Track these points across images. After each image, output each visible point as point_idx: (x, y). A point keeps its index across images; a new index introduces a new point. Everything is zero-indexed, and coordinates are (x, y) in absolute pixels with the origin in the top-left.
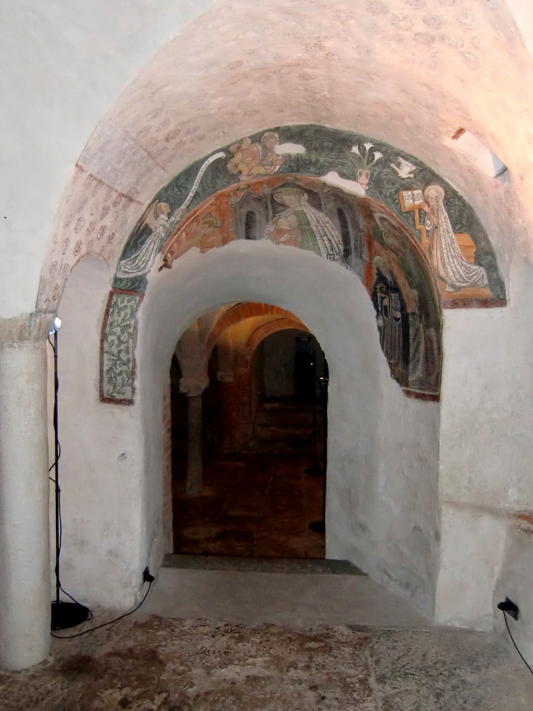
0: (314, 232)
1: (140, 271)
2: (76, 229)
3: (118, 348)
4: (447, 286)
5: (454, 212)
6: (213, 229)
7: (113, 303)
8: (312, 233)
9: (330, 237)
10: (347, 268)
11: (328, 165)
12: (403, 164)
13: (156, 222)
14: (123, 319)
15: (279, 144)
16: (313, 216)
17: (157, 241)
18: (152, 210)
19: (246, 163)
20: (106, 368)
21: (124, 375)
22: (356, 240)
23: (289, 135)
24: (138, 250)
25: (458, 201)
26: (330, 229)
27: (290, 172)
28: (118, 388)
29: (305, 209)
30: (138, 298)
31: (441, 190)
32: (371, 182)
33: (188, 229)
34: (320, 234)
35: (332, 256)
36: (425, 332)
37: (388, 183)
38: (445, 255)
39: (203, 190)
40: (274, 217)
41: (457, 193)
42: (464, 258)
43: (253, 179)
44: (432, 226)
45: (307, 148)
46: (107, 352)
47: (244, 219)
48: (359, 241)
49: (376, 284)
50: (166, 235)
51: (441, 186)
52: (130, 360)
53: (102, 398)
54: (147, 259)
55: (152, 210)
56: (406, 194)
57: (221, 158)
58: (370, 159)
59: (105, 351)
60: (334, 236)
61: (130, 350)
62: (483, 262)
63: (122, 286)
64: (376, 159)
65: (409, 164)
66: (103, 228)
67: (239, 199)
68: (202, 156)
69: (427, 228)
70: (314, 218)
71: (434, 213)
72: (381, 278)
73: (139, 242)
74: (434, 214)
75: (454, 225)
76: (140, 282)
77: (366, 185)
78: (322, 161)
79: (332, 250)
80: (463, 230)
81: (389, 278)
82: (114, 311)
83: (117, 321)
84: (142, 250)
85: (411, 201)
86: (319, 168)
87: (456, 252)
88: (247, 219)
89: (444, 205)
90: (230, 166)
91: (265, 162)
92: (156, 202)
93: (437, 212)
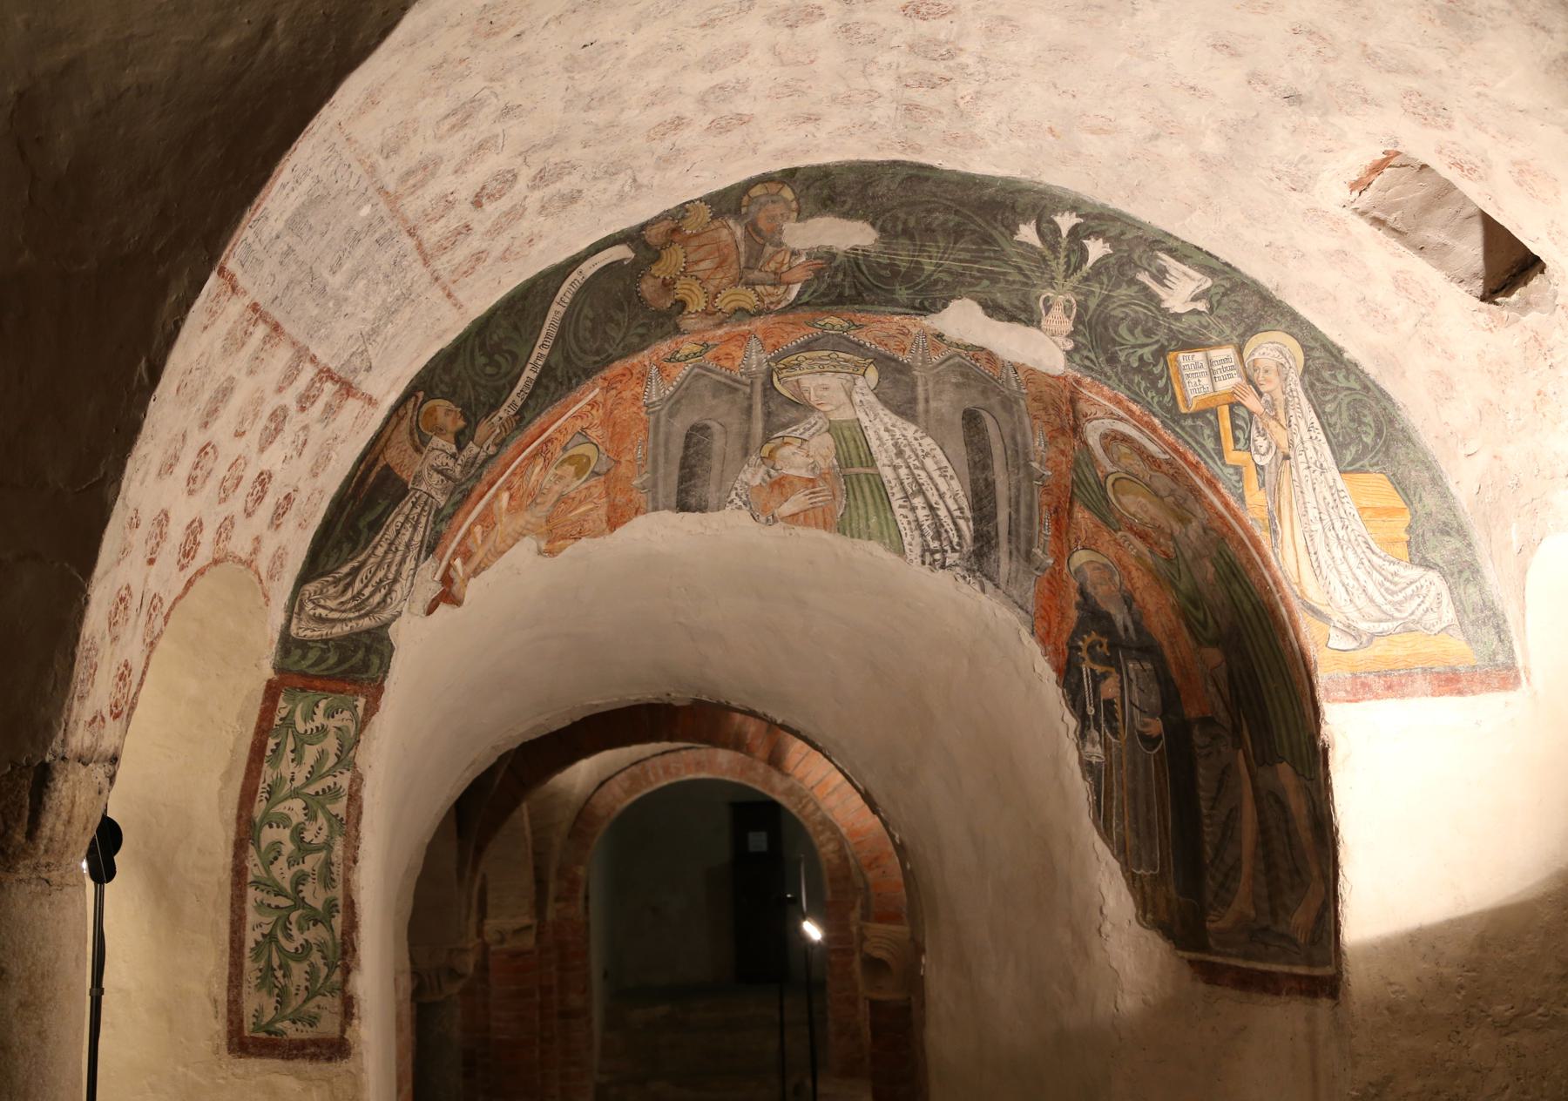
0: (886, 483)
1: (367, 615)
2: (192, 479)
3: (295, 869)
4: (1332, 632)
5: (1335, 410)
6: (586, 481)
7: (277, 721)
8: (879, 486)
9: (934, 499)
10: (983, 590)
11: (949, 279)
12: (1173, 272)
13: (419, 459)
14: (310, 772)
15: (798, 220)
16: (886, 436)
17: (423, 520)
18: (405, 425)
19: (697, 279)
20: (251, 937)
21: (316, 957)
22: (1015, 504)
23: (826, 192)
24: (359, 548)
25: (1347, 378)
26: (936, 475)
27: (832, 303)
28: (295, 1002)
29: (862, 416)
30: (361, 702)
31: (1293, 346)
32: (1081, 327)
33: (516, 481)
34: (904, 489)
35: (937, 556)
36: (1253, 777)
37: (1132, 332)
38: (1319, 538)
39: (567, 359)
40: (767, 440)
41: (1340, 351)
42: (1373, 545)
43: (719, 325)
44: (1271, 454)
45: (882, 230)
46: (257, 883)
47: (677, 451)
48: (1023, 509)
49: (1077, 634)
50: (453, 501)
51: (1292, 335)
52: (336, 905)
53: (235, 1040)
54: (391, 576)
55: (405, 425)
56: (1189, 362)
57: (621, 261)
58: (1073, 260)
59: (250, 878)
60: (947, 496)
61: (338, 870)
62: (1434, 557)
63: (309, 662)
64: (1090, 262)
65: (1191, 272)
66: (264, 479)
67: (671, 389)
68: (561, 257)
69: (1257, 458)
70: (891, 442)
71: (1276, 415)
72: (1093, 616)
73: (362, 524)
74: (1275, 418)
75: (1337, 448)
76: (368, 649)
77: (1068, 336)
78: (929, 268)
79: (938, 536)
80: (1366, 462)
81: (1120, 616)
82: (282, 746)
83: (292, 779)
84: (375, 548)
85: (1205, 381)
86: (921, 290)
87: (1349, 529)
88: (687, 447)
89: (1306, 391)
90: (648, 287)
91: (755, 275)
92: (417, 397)
93: (1286, 413)
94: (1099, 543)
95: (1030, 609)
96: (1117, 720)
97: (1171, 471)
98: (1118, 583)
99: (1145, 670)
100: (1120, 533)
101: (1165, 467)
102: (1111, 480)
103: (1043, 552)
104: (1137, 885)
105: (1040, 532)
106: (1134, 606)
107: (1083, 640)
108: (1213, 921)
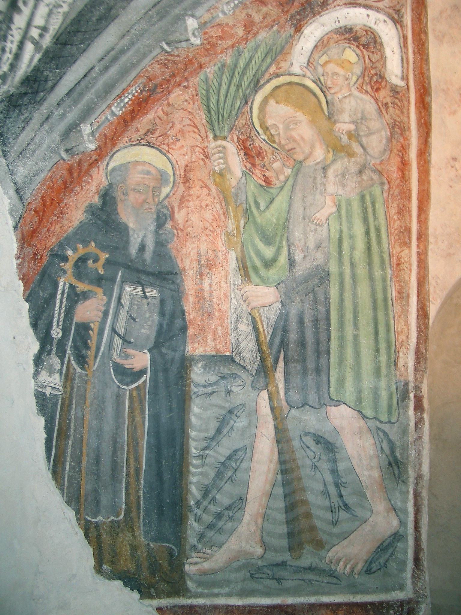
48: (113, 70)
94: (179, 144)
95: (28, 196)
96: (87, 347)
97: (388, 100)
98: (162, 196)
99: (146, 297)
100: (219, 142)
101: (384, 95)
102: (282, 80)
103: (92, 133)
104: (93, 533)
105: (109, 106)
106: (169, 225)
107: (75, 250)
108: (196, 563)
